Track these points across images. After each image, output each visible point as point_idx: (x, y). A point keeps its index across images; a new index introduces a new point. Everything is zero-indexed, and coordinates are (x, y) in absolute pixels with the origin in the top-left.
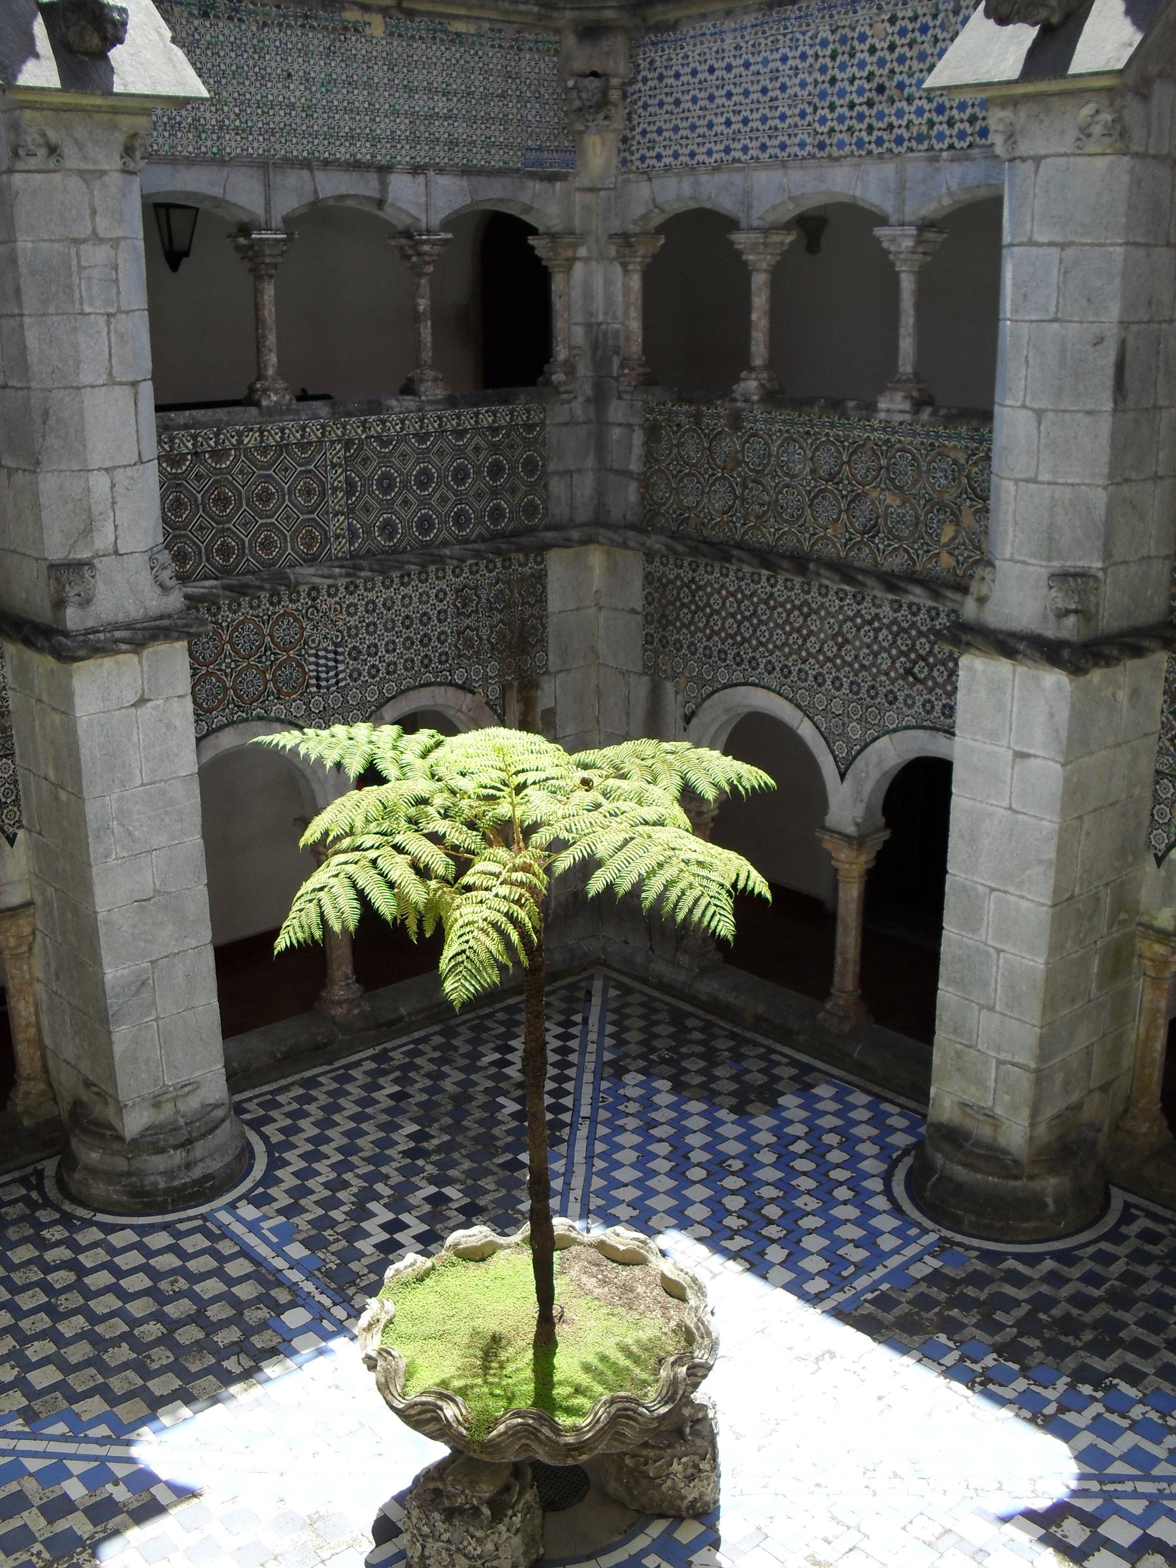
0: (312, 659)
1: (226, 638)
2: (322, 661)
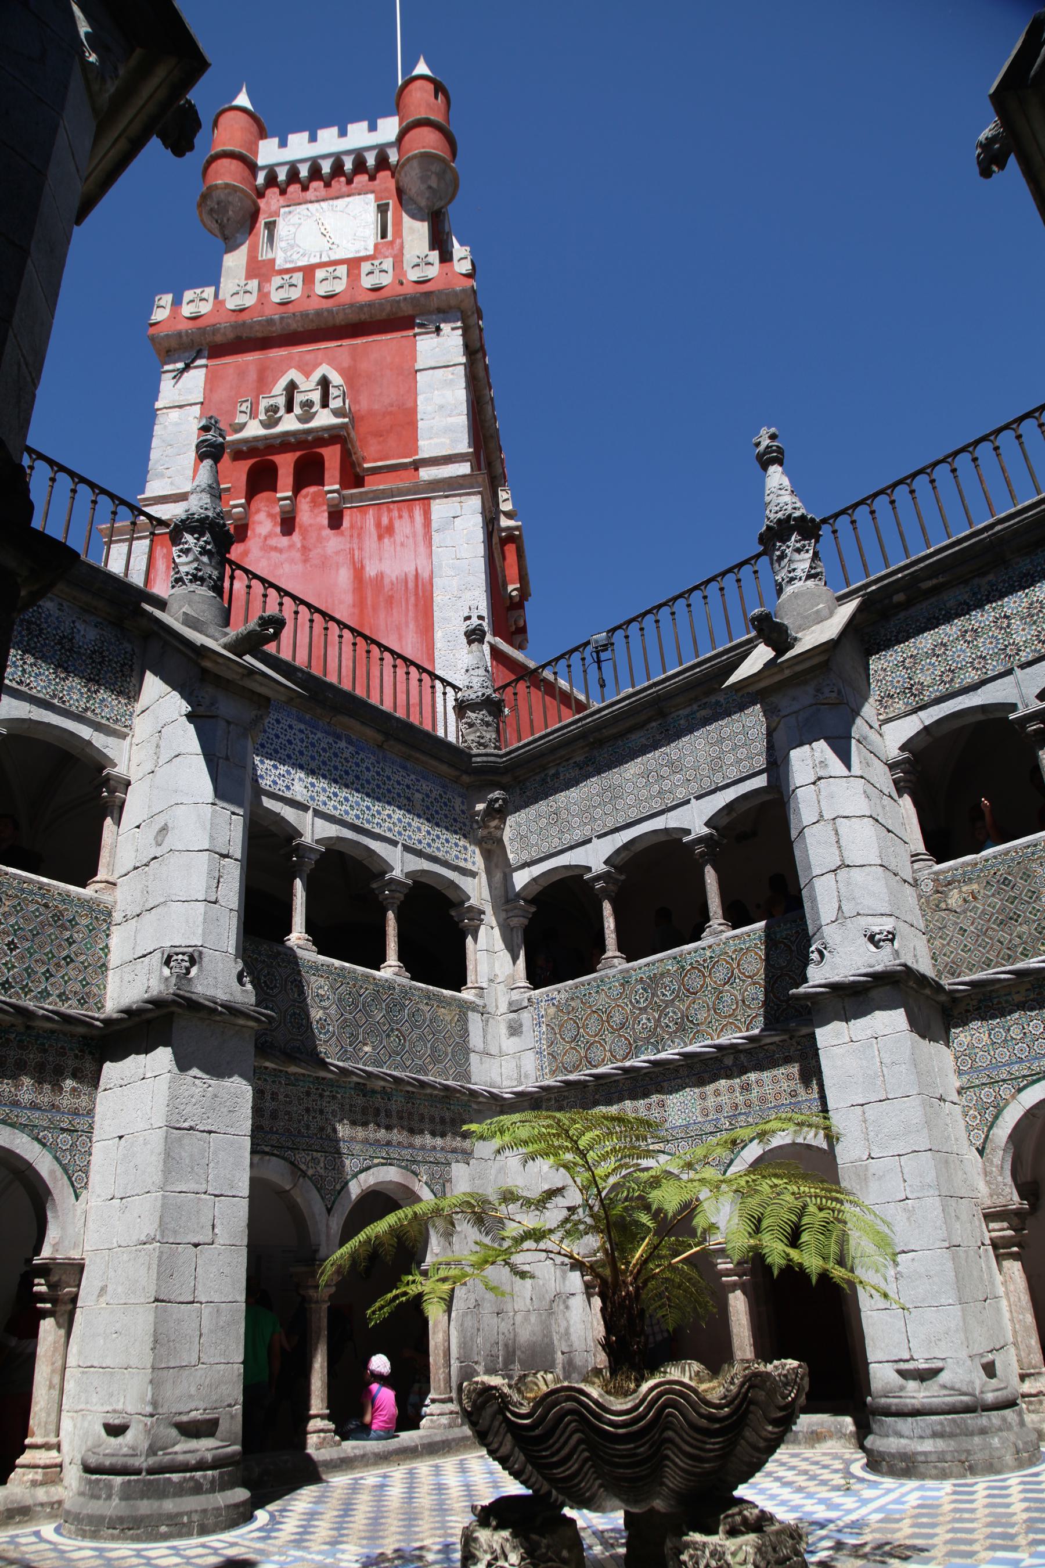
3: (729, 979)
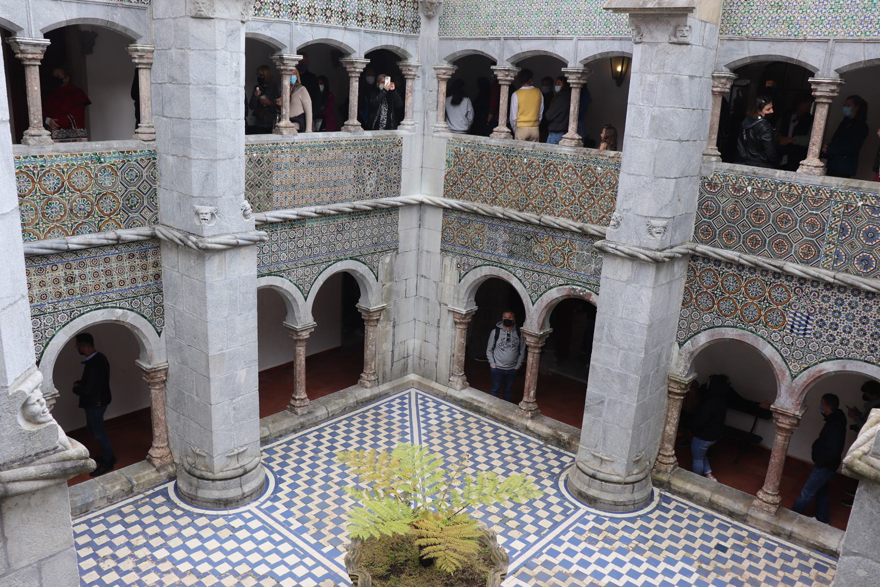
0: (792, 315)
1: (743, 284)
2: (797, 319)
3: (59, 189)
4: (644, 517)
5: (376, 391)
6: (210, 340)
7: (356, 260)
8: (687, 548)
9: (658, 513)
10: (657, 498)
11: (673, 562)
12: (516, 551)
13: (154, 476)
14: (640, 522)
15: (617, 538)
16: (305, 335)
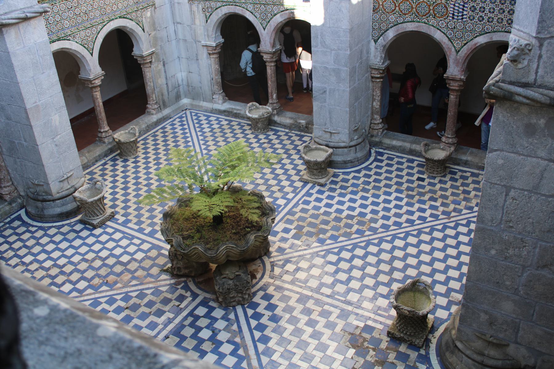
0: (452, 6)
2: (456, 8)
4: (366, 168)
5: (160, 116)
6: (24, 97)
7: (124, 18)
8: (397, 183)
9: (375, 164)
10: (373, 154)
11: (389, 194)
12: (281, 206)
13: (7, 208)
14: (363, 172)
15: (349, 185)
16: (98, 82)
